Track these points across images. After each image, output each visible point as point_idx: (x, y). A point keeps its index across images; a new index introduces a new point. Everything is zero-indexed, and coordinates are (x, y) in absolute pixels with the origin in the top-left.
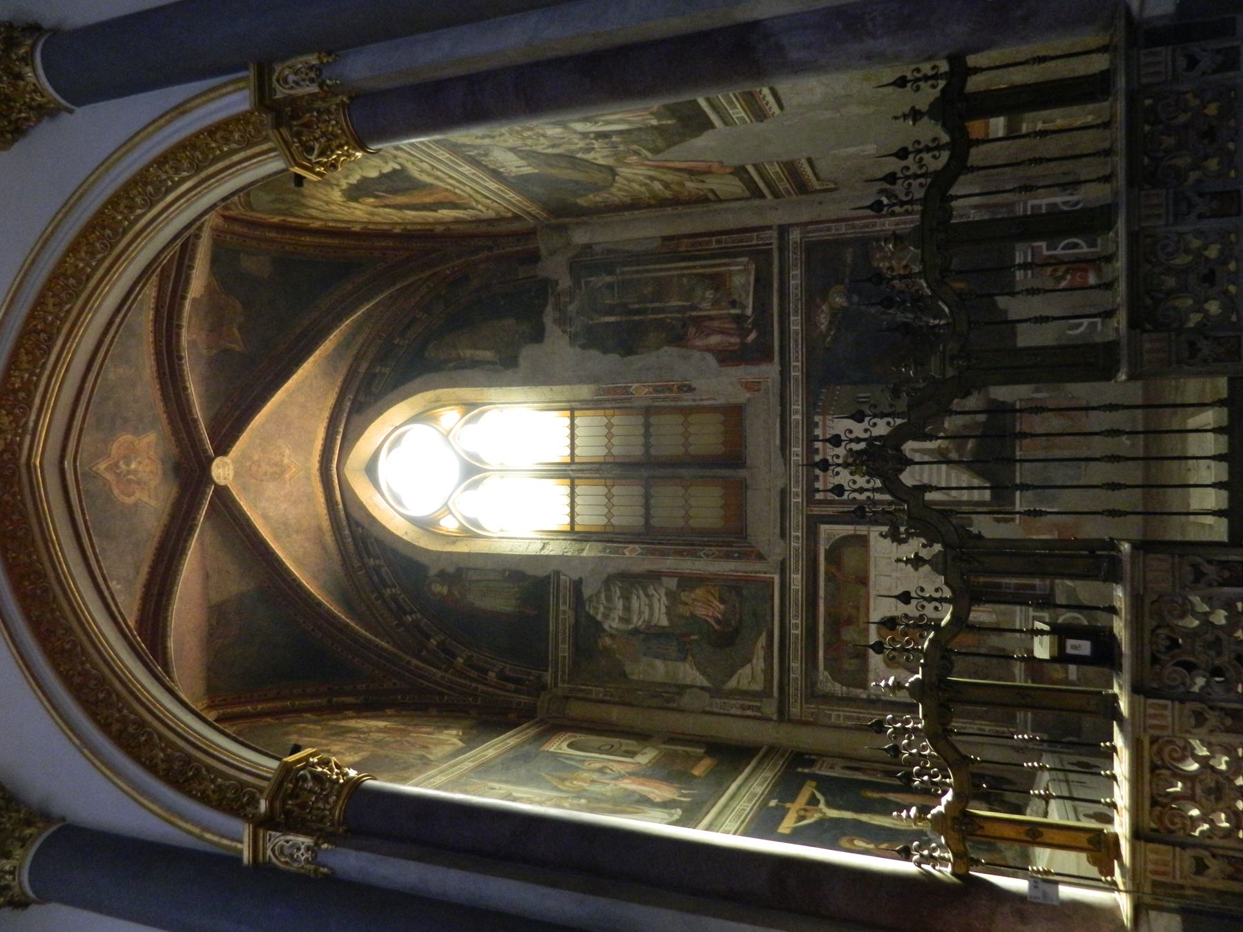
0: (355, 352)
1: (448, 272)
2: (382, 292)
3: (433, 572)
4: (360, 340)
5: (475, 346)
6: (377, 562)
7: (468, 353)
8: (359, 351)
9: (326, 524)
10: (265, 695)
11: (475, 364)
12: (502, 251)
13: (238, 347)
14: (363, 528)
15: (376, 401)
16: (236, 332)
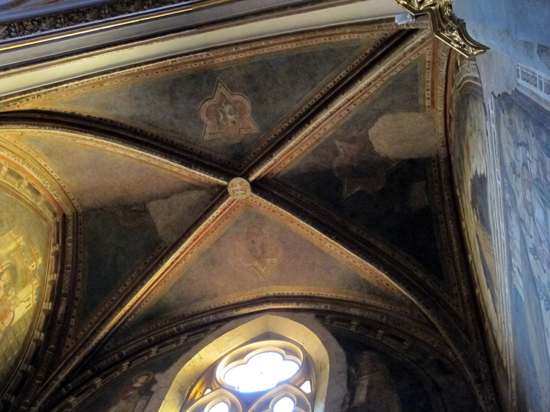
0: (368, 301)
1: (450, 354)
2: (419, 300)
3: (157, 376)
4: (378, 303)
5: (370, 387)
6: (182, 341)
7: (365, 382)
8: (369, 305)
9: (220, 302)
10: (81, 252)
11: (352, 388)
12: (478, 391)
13: (346, 193)
14: (214, 330)
15: (324, 325)
16: (358, 189)
